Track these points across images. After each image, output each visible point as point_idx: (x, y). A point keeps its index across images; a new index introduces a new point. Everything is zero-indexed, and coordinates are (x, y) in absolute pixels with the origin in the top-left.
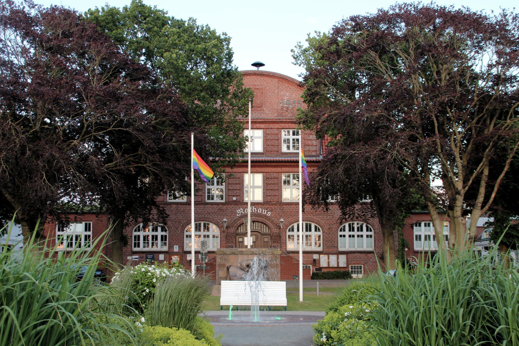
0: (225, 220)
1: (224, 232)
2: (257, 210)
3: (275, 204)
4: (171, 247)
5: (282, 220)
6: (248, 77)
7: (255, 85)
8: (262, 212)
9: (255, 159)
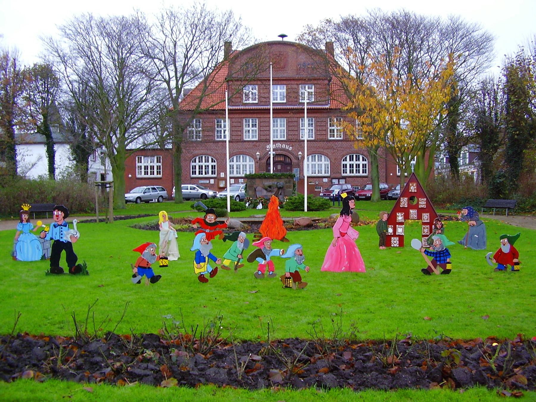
3: (295, 141)
4: (219, 174)
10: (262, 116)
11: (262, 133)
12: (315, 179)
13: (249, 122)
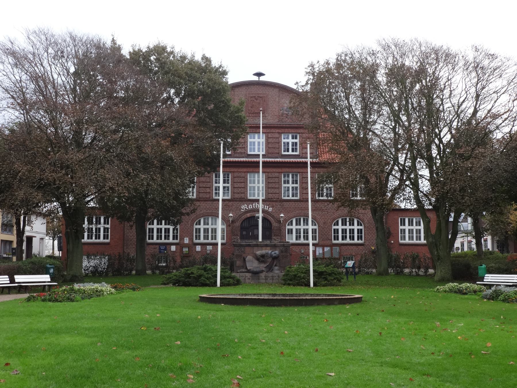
3: (276, 201)
4: (182, 239)
5: (282, 215)
6: (252, 87)
7: (258, 94)
9: (266, 160)
11: (236, 190)
12: (300, 247)
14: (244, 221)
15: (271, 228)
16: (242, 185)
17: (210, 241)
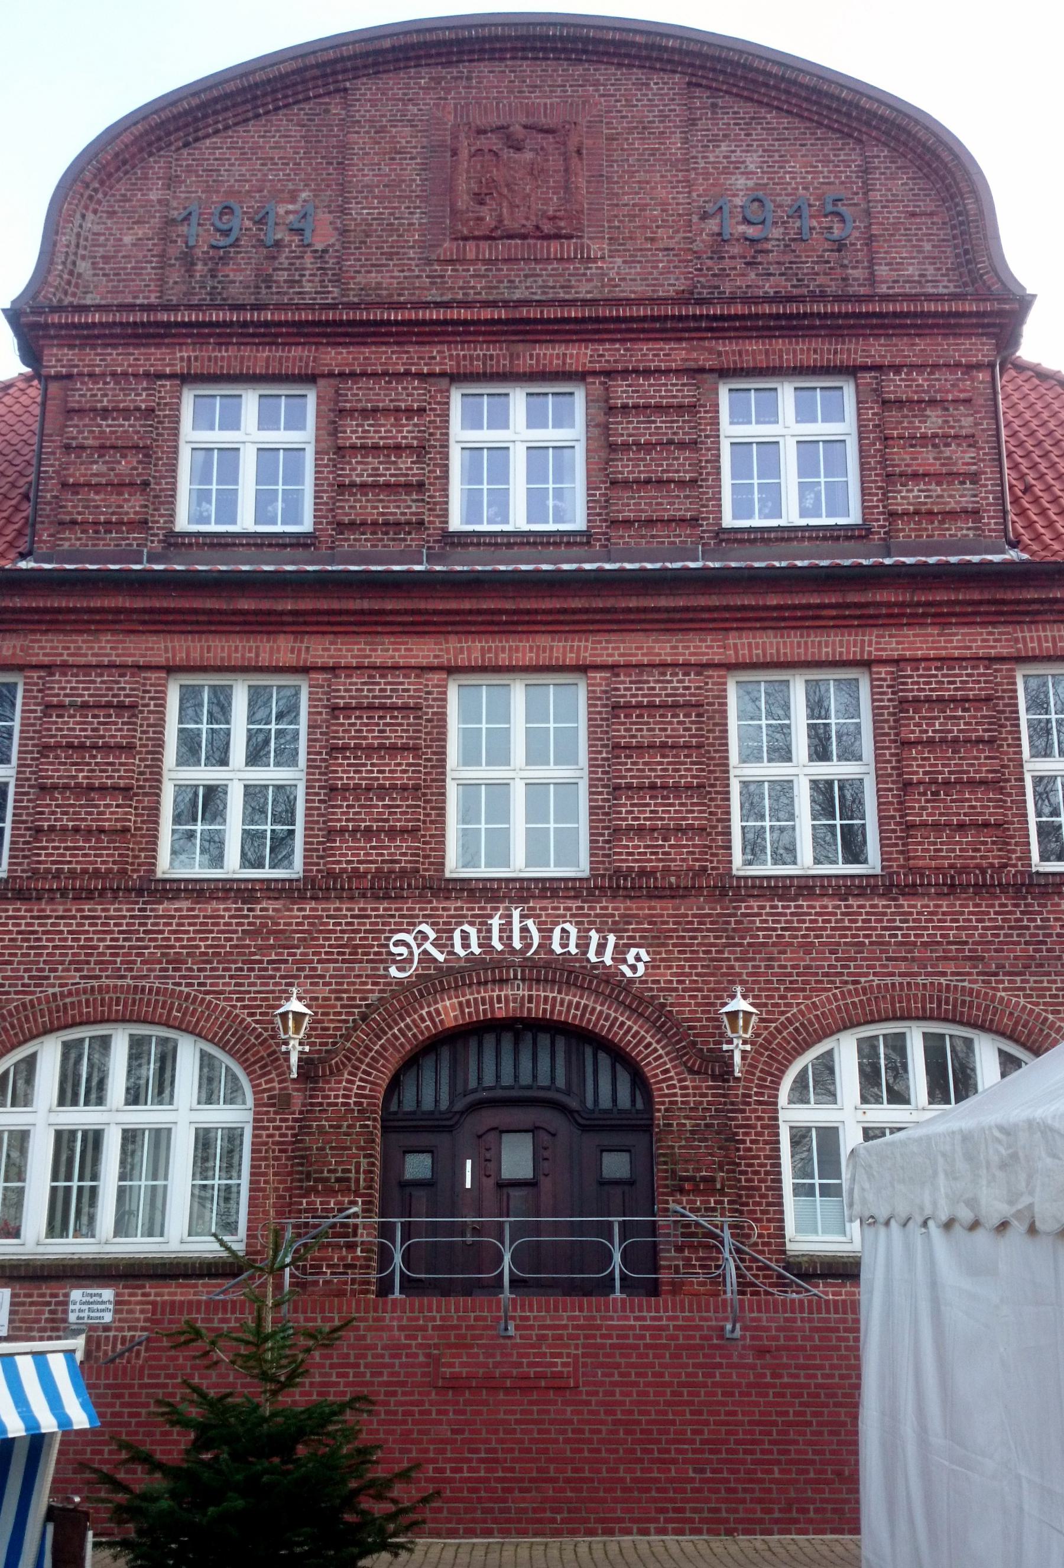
0: (295, 1005)
1: (282, 1102)
2: (546, 933)
5: (740, 1004)
6: (484, 68)
7: (529, 111)
8: (583, 946)
10: (348, 651)
13: (222, 709)
14: (412, 1062)
15: (647, 1128)
16: (399, 770)
17: (104, 1240)
